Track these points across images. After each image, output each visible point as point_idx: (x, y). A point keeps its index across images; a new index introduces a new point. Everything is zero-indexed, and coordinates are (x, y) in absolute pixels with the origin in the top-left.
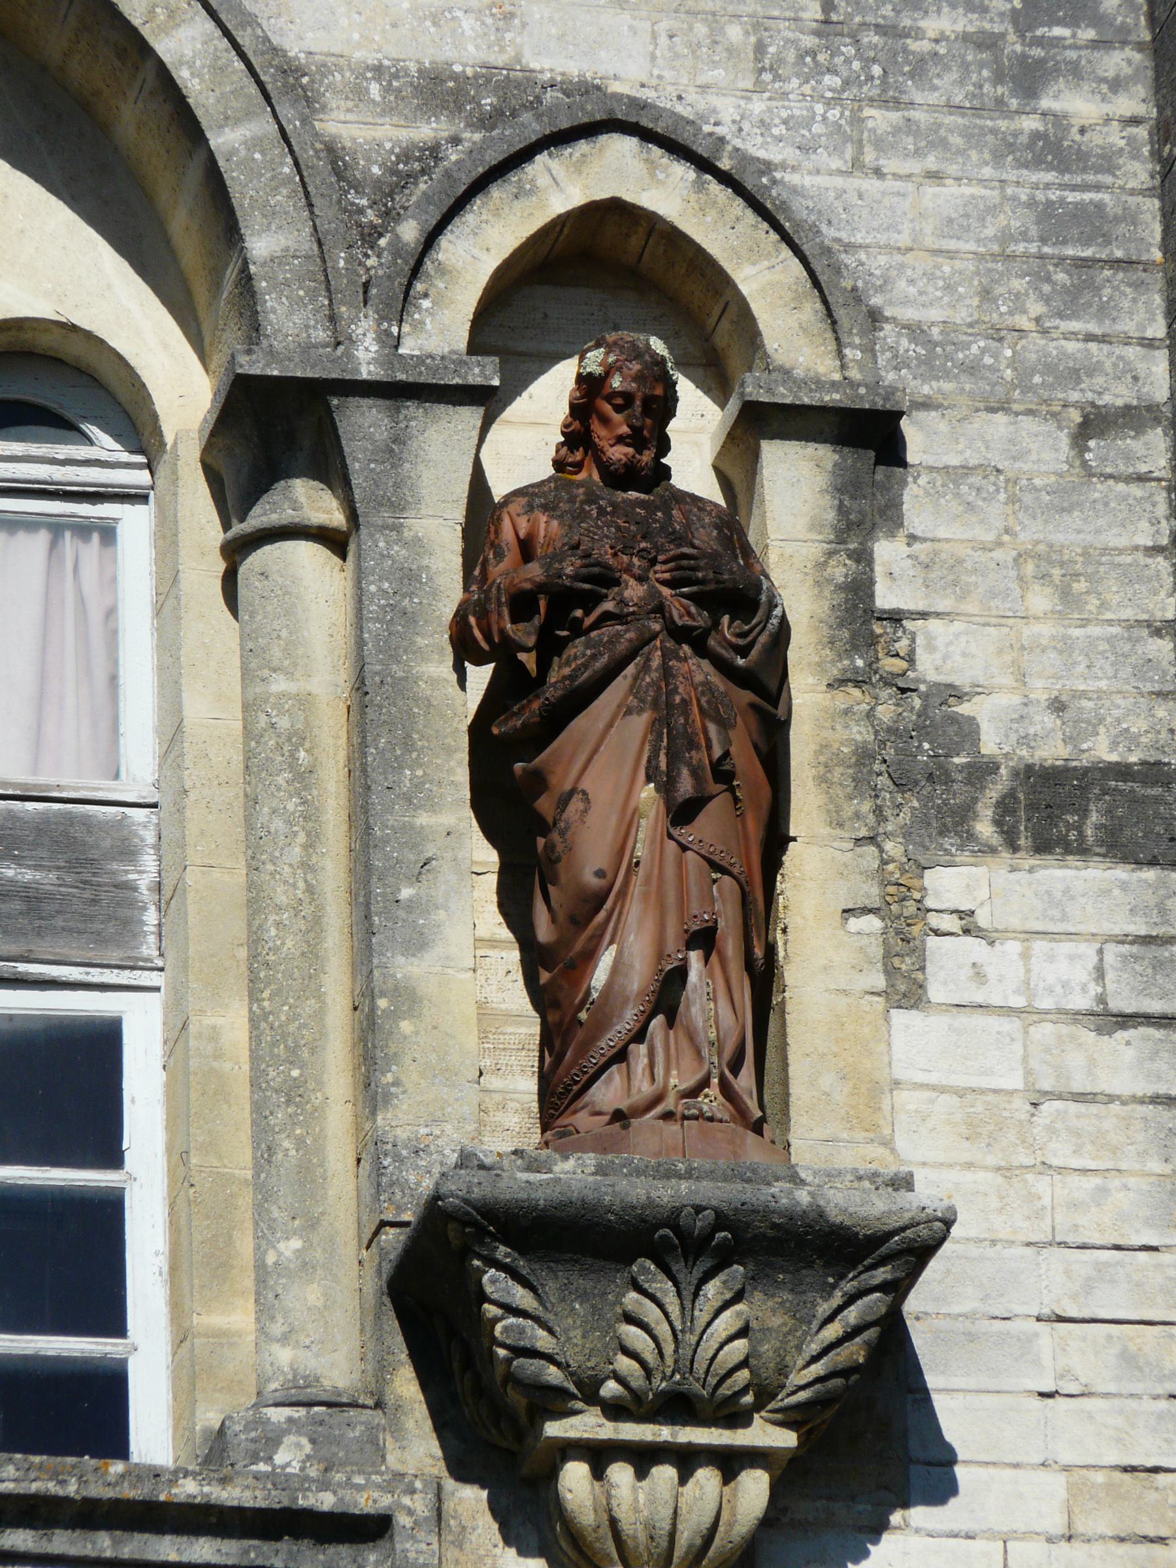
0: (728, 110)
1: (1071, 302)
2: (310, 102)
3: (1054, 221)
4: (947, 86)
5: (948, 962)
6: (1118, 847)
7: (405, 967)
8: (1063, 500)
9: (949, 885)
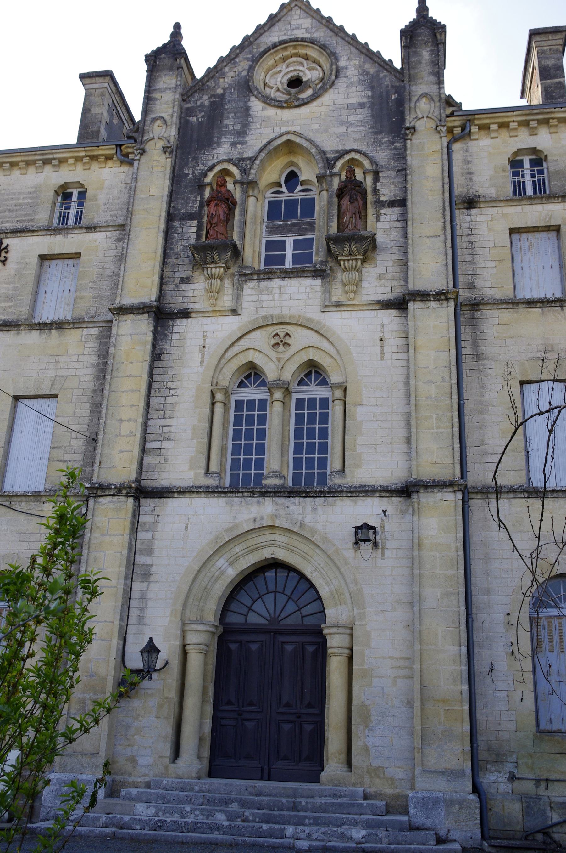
0: (364, 149)
1: (396, 161)
2: (325, 154)
3: (395, 154)
4: (385, 145)
5: (383, 218)
6: (399, 206)
7: (331, 224)
8: (395, 178)
9: (383, 211)
